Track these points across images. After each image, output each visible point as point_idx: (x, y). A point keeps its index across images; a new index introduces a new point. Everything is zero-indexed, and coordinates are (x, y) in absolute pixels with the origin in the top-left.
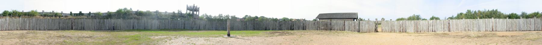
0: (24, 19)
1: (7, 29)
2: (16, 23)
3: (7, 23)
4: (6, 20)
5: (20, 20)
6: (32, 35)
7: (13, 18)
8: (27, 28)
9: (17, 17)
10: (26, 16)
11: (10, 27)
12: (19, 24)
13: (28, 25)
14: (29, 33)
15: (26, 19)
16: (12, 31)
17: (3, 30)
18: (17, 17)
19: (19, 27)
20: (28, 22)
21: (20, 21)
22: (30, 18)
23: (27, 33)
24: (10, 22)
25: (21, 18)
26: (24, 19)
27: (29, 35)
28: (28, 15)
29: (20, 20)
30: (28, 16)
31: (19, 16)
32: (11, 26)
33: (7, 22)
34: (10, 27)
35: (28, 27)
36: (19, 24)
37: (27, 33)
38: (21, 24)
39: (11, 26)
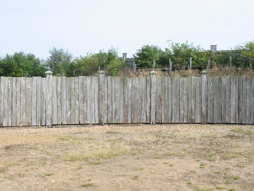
0: (217, 77)
1: (153, 119)
2: (187, 95)
3: (153, 95)
4: (148, 83)
5: (204, 85)
6: (248, 144)
7: (177, 76)
8: (232, 114)
9: (190, 71)
10: (227, 68)
11: (162, 110)
12: (198, 99)
13: (234, 102)
14: (239, 137)
15: (225, 80)
16: (173, 127)
17: (137, 124)
18: (190, 71)
19: (198, 111)
20: (234, 89)
21: (201, 87)
22: (244, 76)
23: (232, 137)
24: (164, 90)
25: (204, 77)
26: (217, 77)
27: (240, 143)
28: (236, 64)
29: (204, 85)
30: (234, 68)
31: (200, 69)
32: (167, 107)
33: (154, 90)
34: (162, 110)
35: (233, 111)
36: (198, 99)
37: (232, 137)
38: (207, 99)
39: (167, 107)
